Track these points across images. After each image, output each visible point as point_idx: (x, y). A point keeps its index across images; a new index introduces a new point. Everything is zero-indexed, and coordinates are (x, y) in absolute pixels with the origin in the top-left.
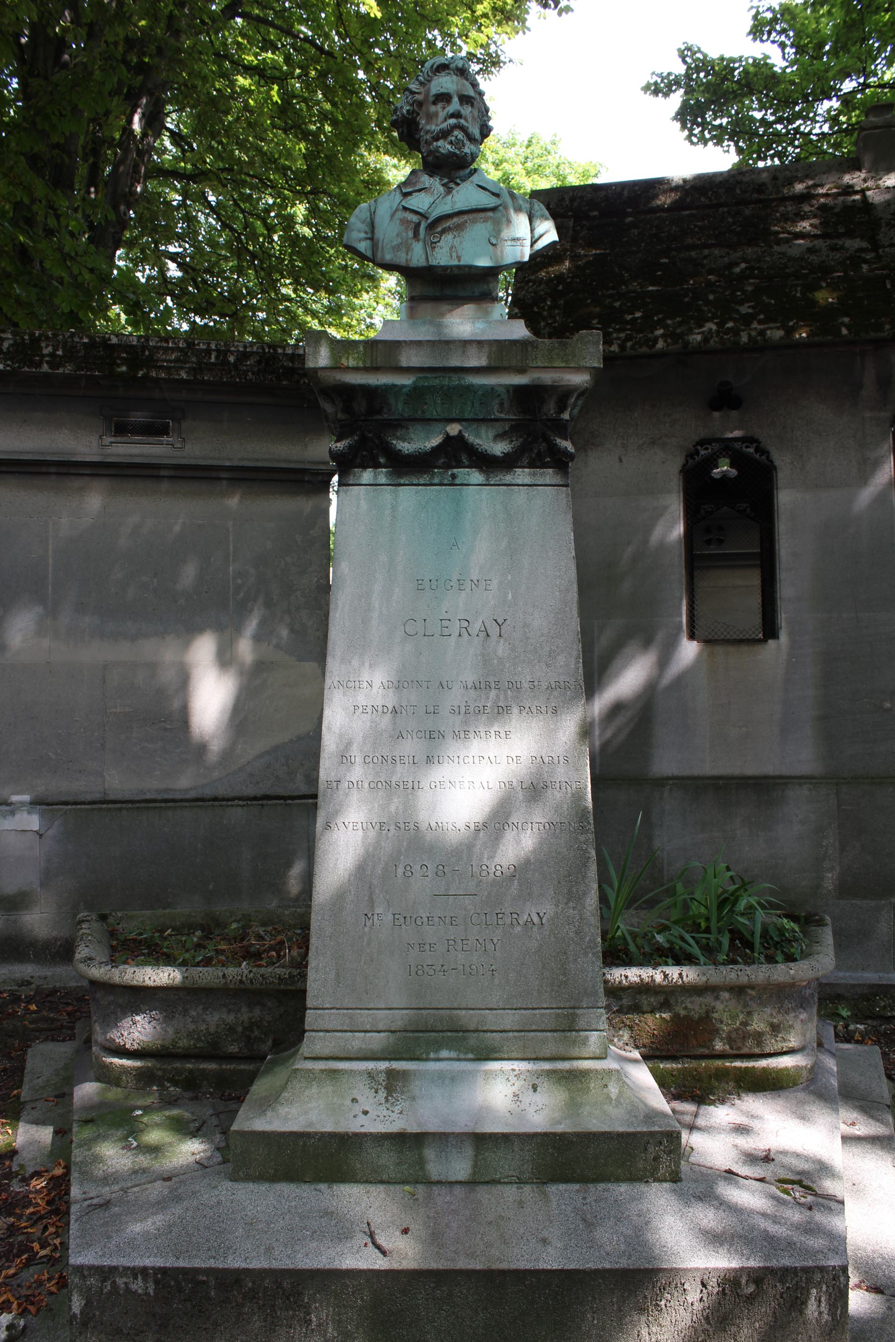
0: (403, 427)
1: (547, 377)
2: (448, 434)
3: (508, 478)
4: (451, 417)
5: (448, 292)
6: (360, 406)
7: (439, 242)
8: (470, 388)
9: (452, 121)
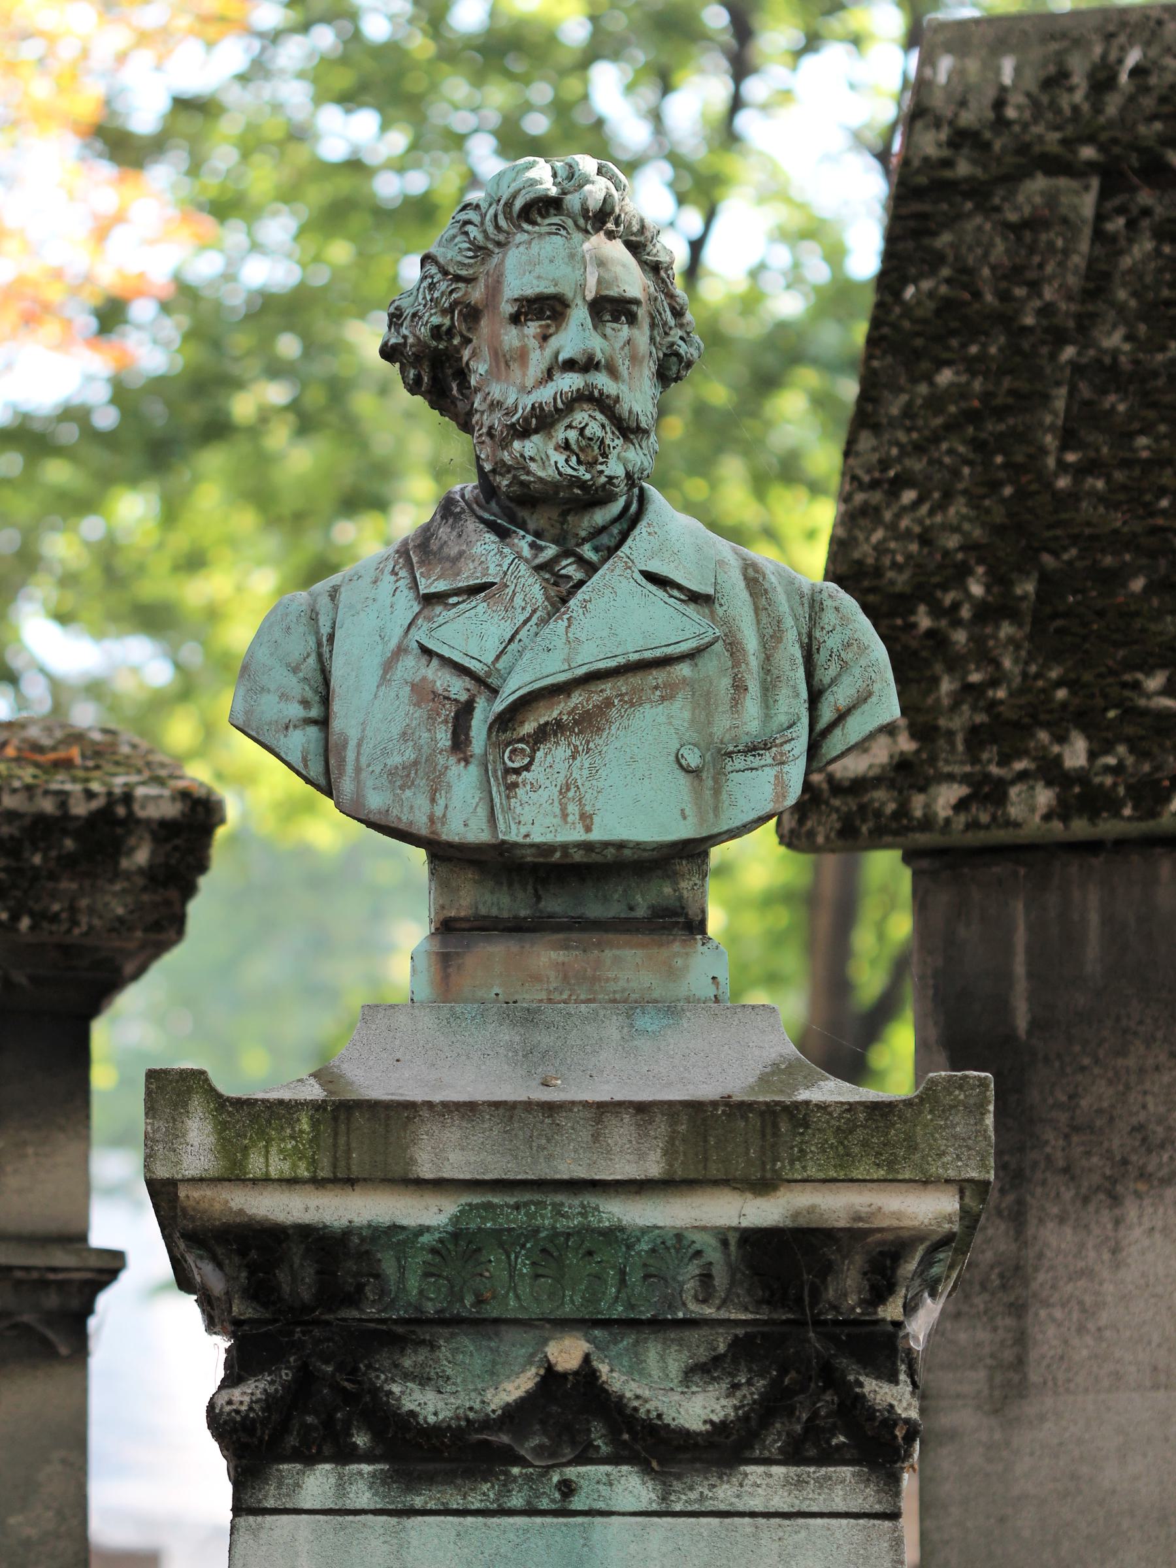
0: (423, 1342)
1: (835, 1205)
2: (550, 1368)
3: (725, 1494)
4: (559, 1314)
5: (555, 904)
6: (299, 1280)
7: (527, 768)
8: (614, 1235)
9: (570, 382)
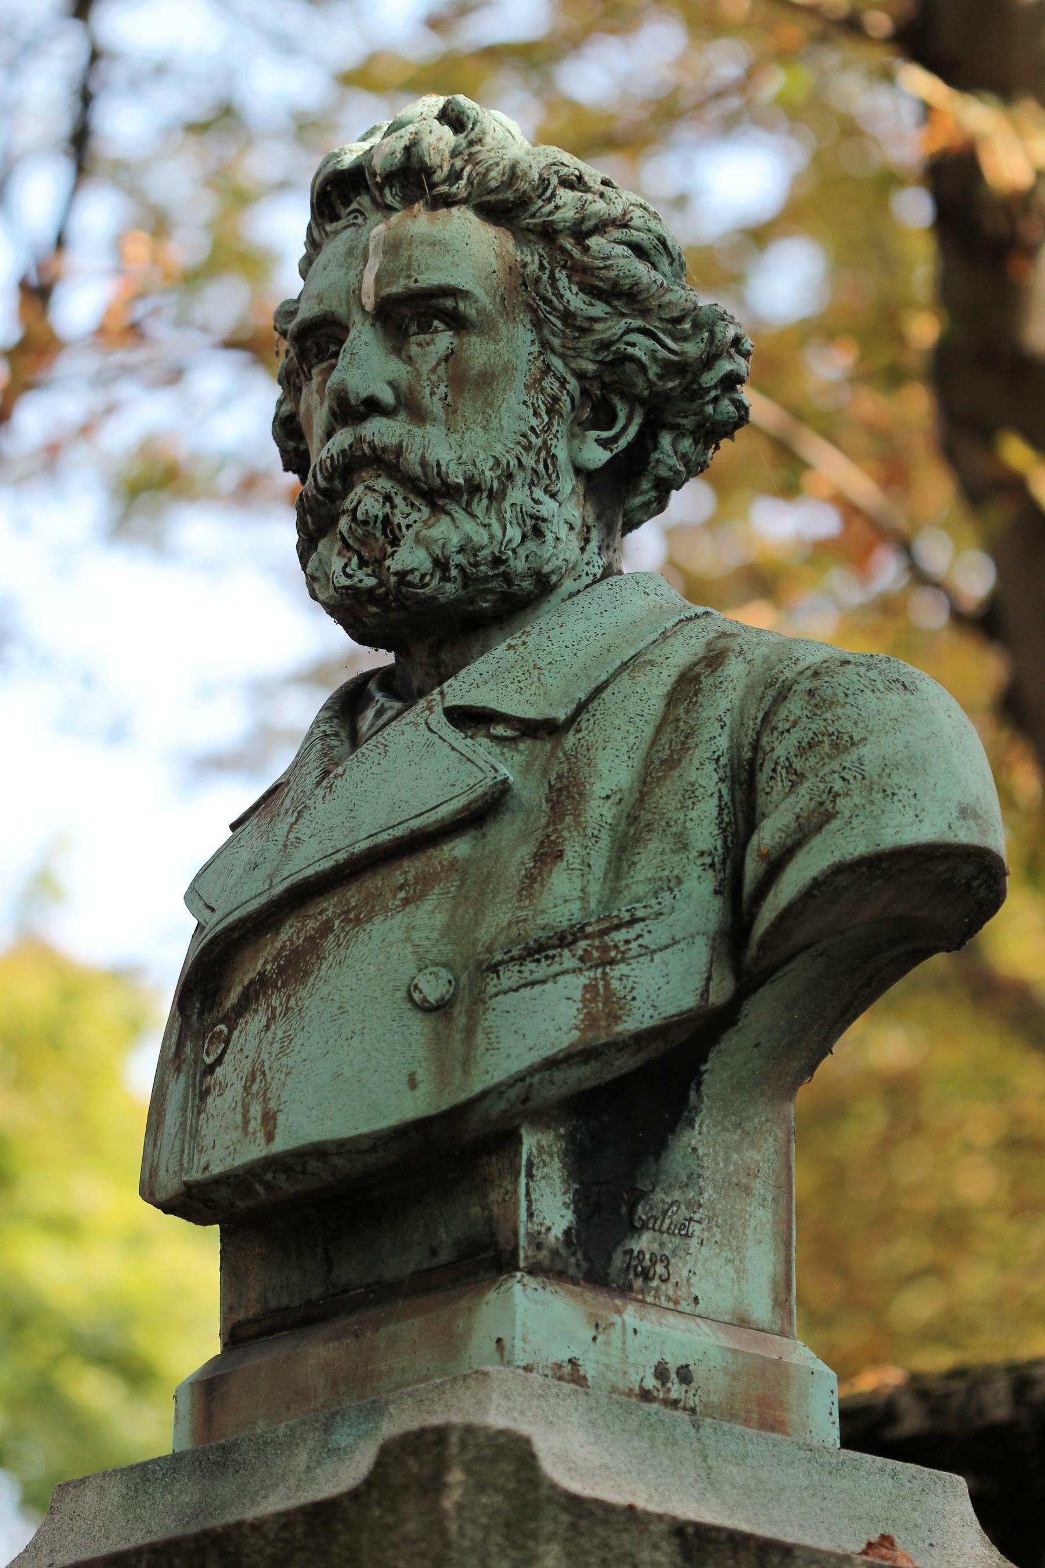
5: (349, 1272)
